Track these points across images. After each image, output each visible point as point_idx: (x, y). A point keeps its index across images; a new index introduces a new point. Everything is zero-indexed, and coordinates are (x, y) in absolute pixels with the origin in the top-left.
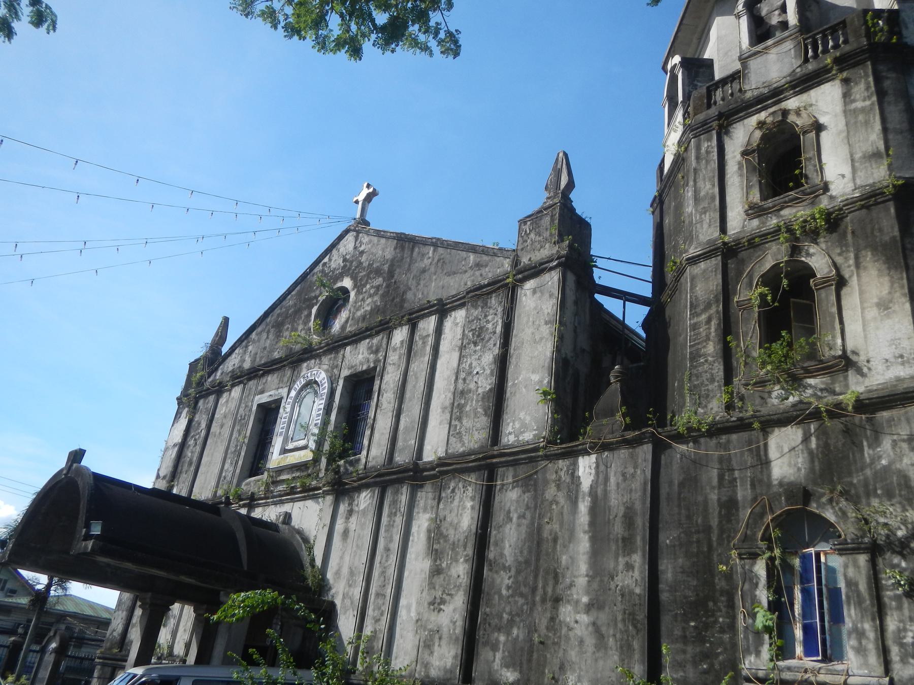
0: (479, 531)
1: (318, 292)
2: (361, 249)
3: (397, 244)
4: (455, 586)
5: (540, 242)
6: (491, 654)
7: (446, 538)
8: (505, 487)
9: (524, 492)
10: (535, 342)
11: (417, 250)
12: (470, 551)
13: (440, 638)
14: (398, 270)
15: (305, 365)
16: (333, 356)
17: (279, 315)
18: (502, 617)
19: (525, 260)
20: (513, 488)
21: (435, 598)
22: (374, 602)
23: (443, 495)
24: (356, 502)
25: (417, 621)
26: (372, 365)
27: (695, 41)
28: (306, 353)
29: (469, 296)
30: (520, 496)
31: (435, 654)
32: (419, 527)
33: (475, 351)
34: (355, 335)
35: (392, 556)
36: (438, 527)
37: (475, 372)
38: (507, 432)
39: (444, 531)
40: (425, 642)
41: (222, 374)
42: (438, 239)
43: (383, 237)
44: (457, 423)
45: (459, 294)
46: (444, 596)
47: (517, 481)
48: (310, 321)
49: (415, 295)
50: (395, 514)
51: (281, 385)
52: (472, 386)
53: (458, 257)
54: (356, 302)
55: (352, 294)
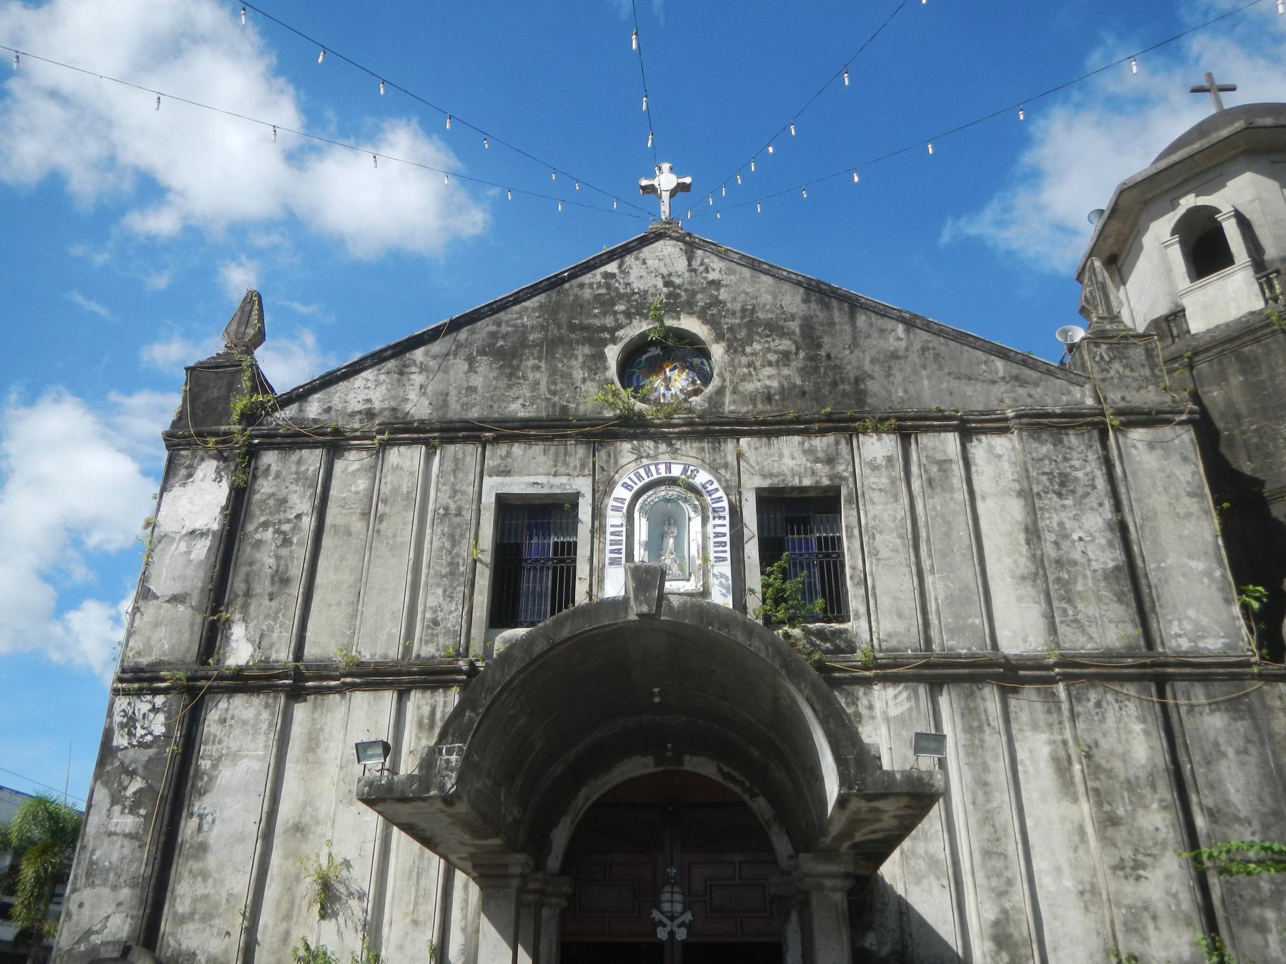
0: (1172, 767)
1: (609, 321)
2: (712, 276)
3: (807, 295)
4: (1156, 844)
5: (1135, 379)
6: (1258, 939)
7: (1110, 773)
8: (1196, 709)
9: (1235, 719)
10: (1179, 516)
11: (862, 320)
12: (1165, 791)
13: (1154, 918)
14: (826, 340)
15: (626, 446)
16: (705, 445)
17: (493, 335)
18: (1258, 888)
19: (1115, 397)
20: (1212, 711)
21: (1122, 860)
22: (984, 865)
23: (1079, 709)
24: (863, 702)
25: (1082, 893)
26: (826, 482)
27: (1179, 180)
28: (627, 426)
29: (1024, 421)
30: (1229, 724)
31: (1154, 941)
32: (1031, 751)
33: (1064, 506)
34: (764, 423)
35: (997, 794)
36: (1089, 756)
37: (1075, 536)
38: (1173, 633)
39: (1103, 763)
40: (1125, 924)
41: (328, 410)
42: (916, 316)
43: (766, 273)
44: (1064, 605)
45: (993, 412)
46: (1140, 857)
47: (1217, 703)
48: (606, 368)
49: (889, 391)
50: (980, 729)
51: (562, 469)
52: (1076, 555)
53: (966, 356)
54: (731, 364)
55: (718, 351)
